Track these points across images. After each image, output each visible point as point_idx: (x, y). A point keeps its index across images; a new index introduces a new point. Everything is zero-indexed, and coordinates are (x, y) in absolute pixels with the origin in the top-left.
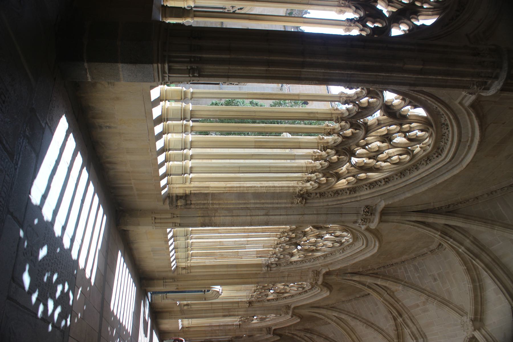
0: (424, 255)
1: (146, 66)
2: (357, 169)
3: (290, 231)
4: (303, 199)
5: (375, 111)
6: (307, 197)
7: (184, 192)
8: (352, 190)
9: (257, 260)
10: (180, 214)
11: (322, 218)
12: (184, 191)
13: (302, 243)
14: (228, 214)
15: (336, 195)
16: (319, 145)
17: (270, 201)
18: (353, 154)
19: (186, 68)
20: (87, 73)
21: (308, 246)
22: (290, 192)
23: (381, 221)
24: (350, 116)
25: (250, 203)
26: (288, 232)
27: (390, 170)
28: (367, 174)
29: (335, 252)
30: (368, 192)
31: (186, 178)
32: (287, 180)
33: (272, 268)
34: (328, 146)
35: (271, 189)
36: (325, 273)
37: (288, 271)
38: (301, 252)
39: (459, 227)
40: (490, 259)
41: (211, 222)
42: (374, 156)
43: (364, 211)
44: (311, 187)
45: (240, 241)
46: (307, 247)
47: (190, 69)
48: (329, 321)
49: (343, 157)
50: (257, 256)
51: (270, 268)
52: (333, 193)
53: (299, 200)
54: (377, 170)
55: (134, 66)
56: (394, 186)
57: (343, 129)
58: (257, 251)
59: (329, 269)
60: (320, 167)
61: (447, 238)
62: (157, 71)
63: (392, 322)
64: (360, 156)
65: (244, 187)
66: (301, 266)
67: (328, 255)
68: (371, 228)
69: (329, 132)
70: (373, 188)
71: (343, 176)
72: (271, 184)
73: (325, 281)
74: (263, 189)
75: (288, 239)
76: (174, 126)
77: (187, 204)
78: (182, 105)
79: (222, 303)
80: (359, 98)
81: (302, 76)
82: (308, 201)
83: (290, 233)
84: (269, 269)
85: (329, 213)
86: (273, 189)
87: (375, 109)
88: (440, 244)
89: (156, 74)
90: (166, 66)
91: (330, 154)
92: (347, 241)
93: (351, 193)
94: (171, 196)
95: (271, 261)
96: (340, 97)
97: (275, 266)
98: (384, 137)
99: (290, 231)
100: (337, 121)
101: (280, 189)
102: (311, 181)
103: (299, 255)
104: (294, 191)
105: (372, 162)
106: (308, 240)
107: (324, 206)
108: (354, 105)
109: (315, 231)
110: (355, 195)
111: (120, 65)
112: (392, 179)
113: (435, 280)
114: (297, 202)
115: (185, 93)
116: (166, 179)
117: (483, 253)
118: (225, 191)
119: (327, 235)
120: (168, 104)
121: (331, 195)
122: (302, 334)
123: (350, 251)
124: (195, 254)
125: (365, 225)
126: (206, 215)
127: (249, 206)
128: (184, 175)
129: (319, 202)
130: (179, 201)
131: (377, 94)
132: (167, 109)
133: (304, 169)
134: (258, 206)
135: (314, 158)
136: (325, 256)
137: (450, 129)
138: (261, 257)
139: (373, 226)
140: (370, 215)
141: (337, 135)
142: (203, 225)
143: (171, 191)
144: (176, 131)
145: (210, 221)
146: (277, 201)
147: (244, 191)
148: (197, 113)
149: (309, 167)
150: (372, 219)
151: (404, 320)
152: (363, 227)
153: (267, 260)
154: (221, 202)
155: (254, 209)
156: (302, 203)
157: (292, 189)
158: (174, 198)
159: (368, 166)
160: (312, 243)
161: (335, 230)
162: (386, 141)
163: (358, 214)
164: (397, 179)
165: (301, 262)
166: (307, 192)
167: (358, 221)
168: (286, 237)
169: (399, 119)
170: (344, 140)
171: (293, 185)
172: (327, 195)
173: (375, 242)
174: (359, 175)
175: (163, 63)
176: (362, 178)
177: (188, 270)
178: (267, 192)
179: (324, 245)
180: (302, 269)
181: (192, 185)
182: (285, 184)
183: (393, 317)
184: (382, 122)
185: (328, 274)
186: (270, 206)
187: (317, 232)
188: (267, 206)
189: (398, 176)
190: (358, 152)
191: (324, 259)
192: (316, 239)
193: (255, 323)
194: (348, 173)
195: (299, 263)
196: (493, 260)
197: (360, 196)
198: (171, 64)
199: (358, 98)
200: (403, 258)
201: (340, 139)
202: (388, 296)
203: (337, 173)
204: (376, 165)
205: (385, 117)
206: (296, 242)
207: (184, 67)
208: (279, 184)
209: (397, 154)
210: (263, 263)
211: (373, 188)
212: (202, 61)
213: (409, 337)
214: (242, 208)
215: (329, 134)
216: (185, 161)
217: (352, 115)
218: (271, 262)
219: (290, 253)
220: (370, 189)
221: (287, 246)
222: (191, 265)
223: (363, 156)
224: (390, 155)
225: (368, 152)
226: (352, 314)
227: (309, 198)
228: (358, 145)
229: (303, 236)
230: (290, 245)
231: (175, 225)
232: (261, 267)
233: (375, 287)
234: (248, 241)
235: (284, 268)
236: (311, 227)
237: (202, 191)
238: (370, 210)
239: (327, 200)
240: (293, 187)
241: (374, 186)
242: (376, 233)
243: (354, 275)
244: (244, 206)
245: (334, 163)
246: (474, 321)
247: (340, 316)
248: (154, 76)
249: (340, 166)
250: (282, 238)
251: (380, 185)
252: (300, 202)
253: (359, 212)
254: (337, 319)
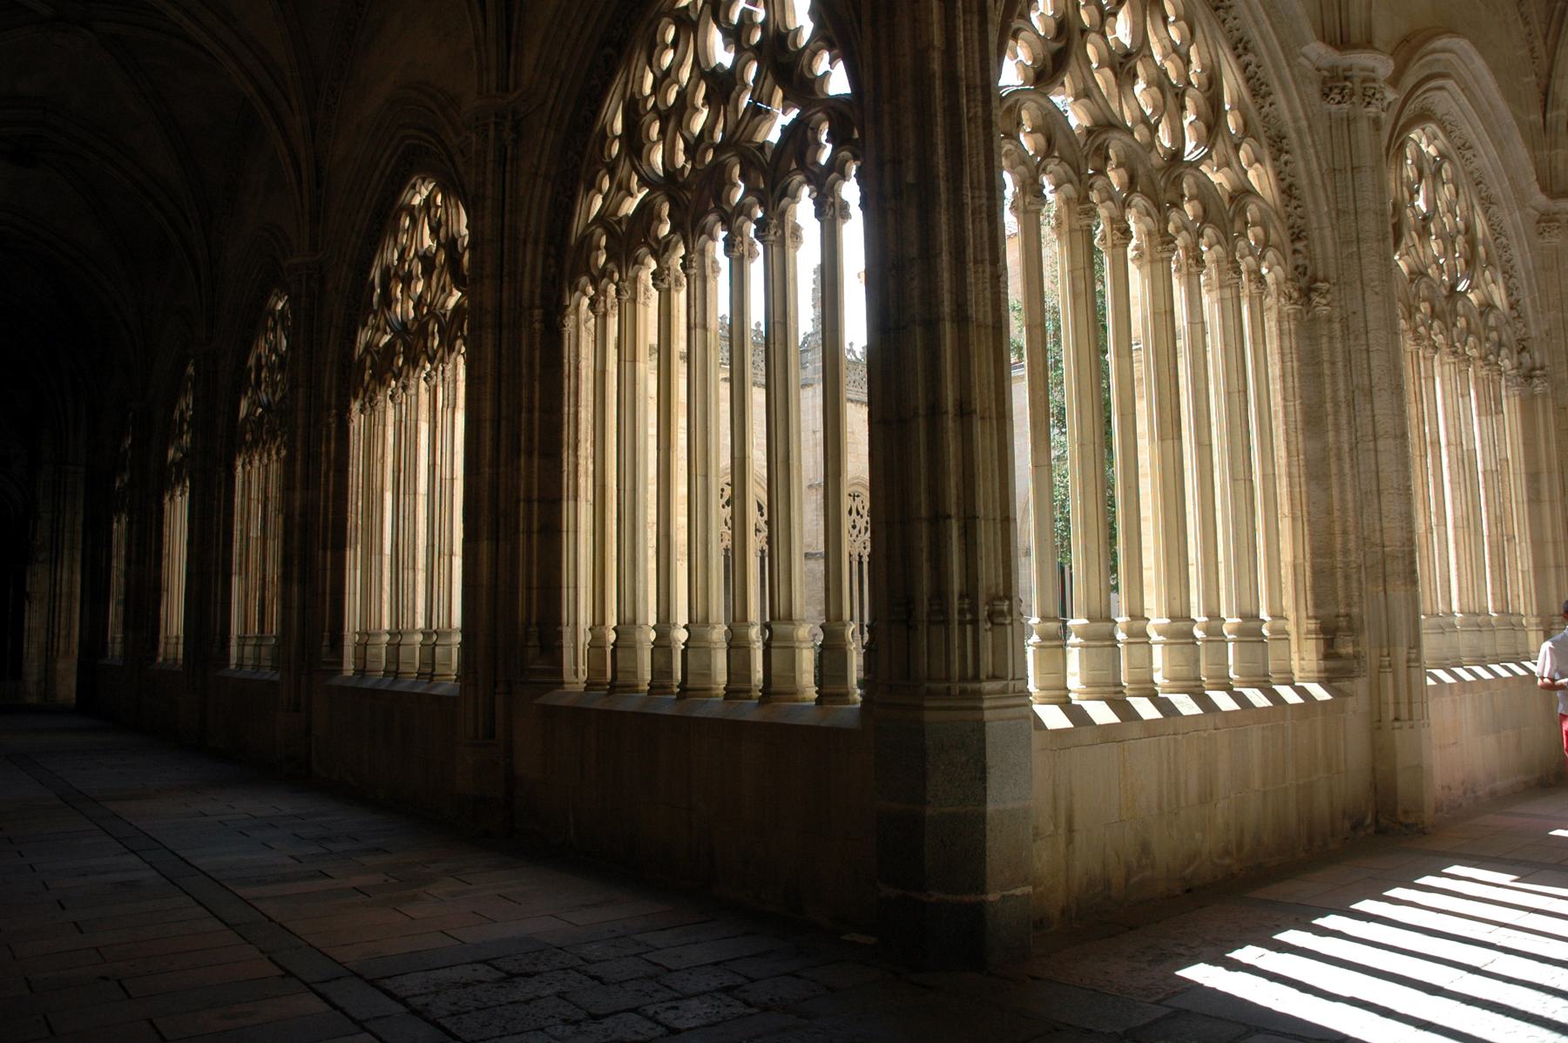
1: (989, 739)
2: (1215, 139)
3: (1410, 317)
4: (1316, 290)
5: (1054, 111)
6: (1307, 278)
7: (1314, 636)
8: (1277, 146)
9: (1509, 413)
10: (1381, 647)
11: (1369, 224)
12: (1309, 636)
13: (1445, 278)
14: (1376, 506)
15: (1295, 192)
16: (1158, 256)
17: (1327, 386)
18: (1176, 156)
19: (989, 633)
20: (1012, 895)
21: (1455, 259)
22: (1296, 330)
23: (1368, 44)
24: (1075, 178)
25: (1338, 441)
26: (1416, 323)
27: (1210, 42)
28: (1227, 107)
29: (1472, 173)
30: (1279, 97)
31: (1272, 631)
32: (1261, 341)
33: (1534, 363)
34: (1159, 230)
35: (1290, 384)
36: (1547, 195)
37: (1542, 313)
38: (1475, 279)
41: (1399, 555)
42: (1177, 94)
43: (1339, 103)
44: (1277, 268)
45: (1450, 467)
46: (1461, 264)
47: (993, 623)
49: (1184, 185)
50: (1496, 413)
51: (1533, 369)
52: (1290, 201)
53: (1318, 299)
54: (1213, 82)
55: (992, 770)
56: (1256, 22)
57: (1109, 195)
58: (1479, 415)
60: (1217, 247)
62: (1002, 711)
64: (1178, 136)
65: (1289, 465)
66: (1523, 275)
67: (1483, 195)
68: (1390, 73)
69: (1122, 234)
70: (1267, 86)
71: (1239, 178)
72: (1276, 387)
74: (1292, 409)
76: (1131, 667)
77: (1350, 629)
78: (1073, 646)
80: (1023, 159)
81: (990, 320)
82: (1320, 275)
83: (1418, 317)
84: (1538, 372)
85: (1352, 206)
86: (1290, 379)
87: (1050, 112)
89: (1010, 713)
90: (988, 686)
91: (1180, 224)
92: (1432, 139)
93: (1286, 147)
94: (1326, 675)
95: (1510, 367)
96: (1026, 212)
97: (1526, 356)
98: (1122, 74)
99: (1410, 317)
101: (1288, 358)
102: (1260, 271)
103: (1487, 285)
104: (1292, 316)
105: (1192, 99)
106: (1436, 261)
107: (1332, 225)
108: (1044, 170)
109: (1406, 244)
111: (991, 807)
112: (1236, 32)
114: (1325, 305)
115: (1045, 637)
116: (1278, 688)
118: (1305, 519)
119: (1416, 203)
120: (1074, 682)
121: (1296, 208)
123: (1468, 126)
124: (1499, 604)
125: (1382, 93)
126: (1380, 570)
127: (1346, 447)
128: (1266, 637)
129: (1323, 242)
130: (1343, 651)
131: (1010, 110)
132: (1088, 685)
133: (1228, 293)
134: (1343, 421)
135: (1193, 270)
136: (1487, 202)
138: (1498, 402)
139: (1383, 66)
140: (1351, 82)
141: (1127, 210)
142: (1411, 578)
143: (1311, 675)
144: (1147, 661)
145: (1397, 557)
146: (1326, 366)
147: (1302, 463)
148: (1095, 605)
149: (1220, 281)
150: (1362, 74)
152: (1391, 95)
153: (1507, 380)
154: (1337, 528)
155: (1353, 430)
156: (1328, 291)
157: (1286, 326)
158: (1331, 664)
159: (1203, 109)
160: (1445, 248)
161: (1402, 183)
162: (1130, 68)
163: (1350, 121)
164: (1235, 19)
165: (1511, 277)
166: (1292, 280)
167: (1371, 115)
168: (1431, 327)
169: (1068, 40)
170: (1139, 189)
171: (1273, 324)
172: (1299, 221)
173: (1434, 51)
174: (1233, 132)
175: (978, 695)
176: (1240, 121)
177: (1552, 624)
178: (1301, 398)
179: (1449, 211)
180: (1534, 268)
181: (1291, 615)
182: (1273, 346)
184: (1082, 86)
186: (1341, 385)
187: (1410, 238)
188: (1342, 394)
189: (1225, 16)
190: (1167, 144)
191: (1495, 204)
192: (1433, 237)
194: (1228, 165)
195: (1513, 280)
197: (1295, 120)
198: (983, 676)
199: (1023, 163)
201: (1138, 200)
203: (1232, 198)
204: (1199, 84)
205: (1067, 80)
206: (1446, 297)
207: (987, 639)
208: (1275, 364)
209: (1163, 29)
210: (1517, 393)
211: (1267, 86)
212: (970, 592)
214: (1352, 467)
216: (1225, 632)
217: (1071, 173)
218: (1512, 369)
219: (1481, 314)
220: (1270, 94)
221: (1458, 325)
222: (1535, 612)
223: (1179, 124)
224: (1171, 50)
225: (1165, 115)
227: (1309, 272)
228: (1151, 145)
229: (1425, 279)
230: (1455, 314)
231: (1414, 661)
232: (1533, 396)
234: (1448, 444)
235: (1532, 326)
236: (1396, 257)
237: (1308, 584)
238: (1334, 84)
239: (1313, 218)
240: (1279, 321)
241: (1262, 84)
244: (1347, 460)
245: (1205, 210)
248: (1014, 719)
249: (1213, 190)
250: (1435, 342)
251: (1259, 67)
252: (1324, 297)
253: (1345, 116)
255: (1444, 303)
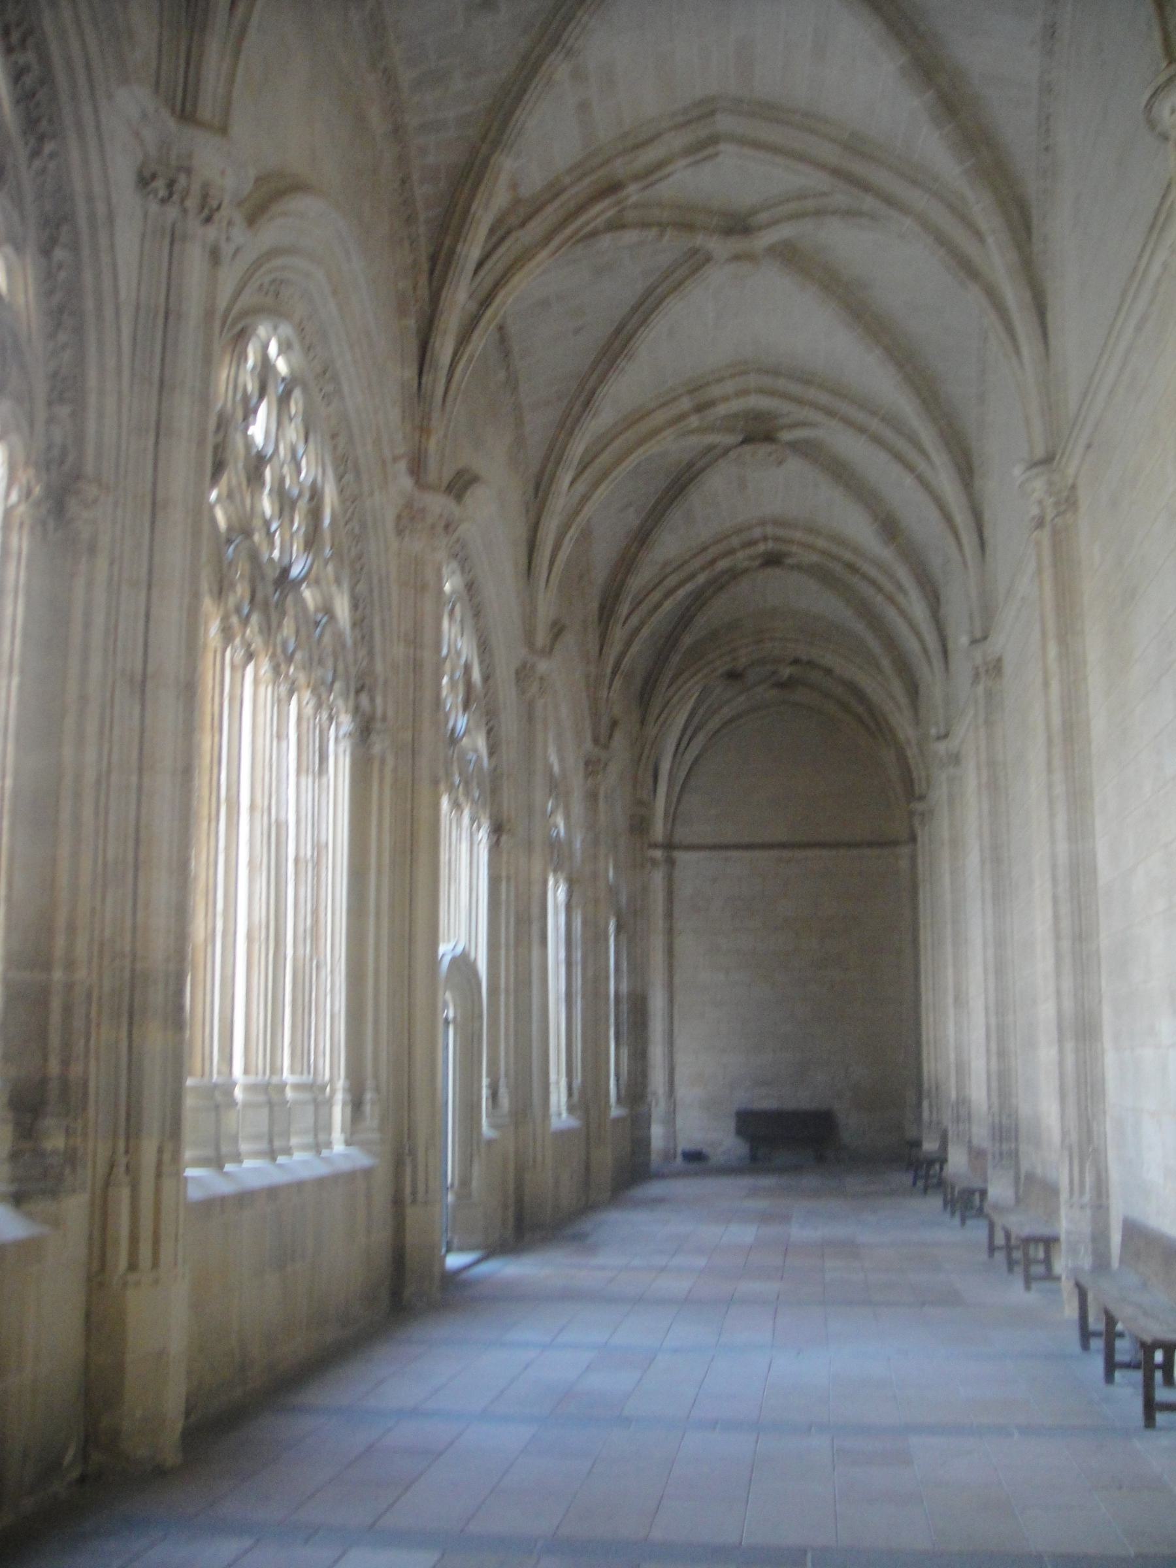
59: (395, 459)
75: (255, 618)
97: (364, 699)
127: (90, 776)
134: (92, 728)
138: (323, 758)
185: (417, 466)
187: (234, 474)
202: (532, 225)
243: (428, 354)
247: (576, 462)
254: (586, 474)
255: (271, 589)
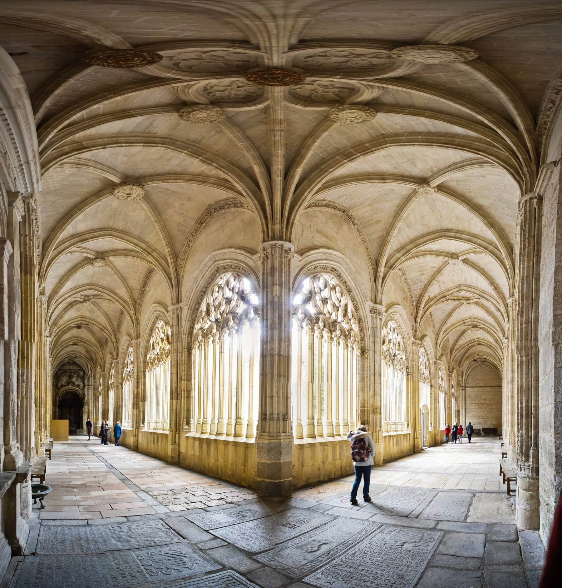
0: (406, 279)
11: (378, 340)
23: (381, 304)
39: (387, 259)
40: (411, 245)
48: (446, 338)
54: (346, 306)
61: (394, 266)
63: (450, 301)
73: (419, 338)
79: (431, 403)
88: (399, 269)
100: (314, 332)
110: (363, 319)
113: (423, 274)
117: (407, 247)
122: (453, 355)
137: (318, 265)
151: (449, 295)
163: (375, 318)
183: (446, 300)
193: (444, 384)
196: (411, 243)
197: (364, 316)
200: (406, 290)
213: (460, 294)
215: (322, 336)
226: (442, 324)
233: (425, 309)
238: (373, 311)
242: (390, 306)
246: (452, 258)
